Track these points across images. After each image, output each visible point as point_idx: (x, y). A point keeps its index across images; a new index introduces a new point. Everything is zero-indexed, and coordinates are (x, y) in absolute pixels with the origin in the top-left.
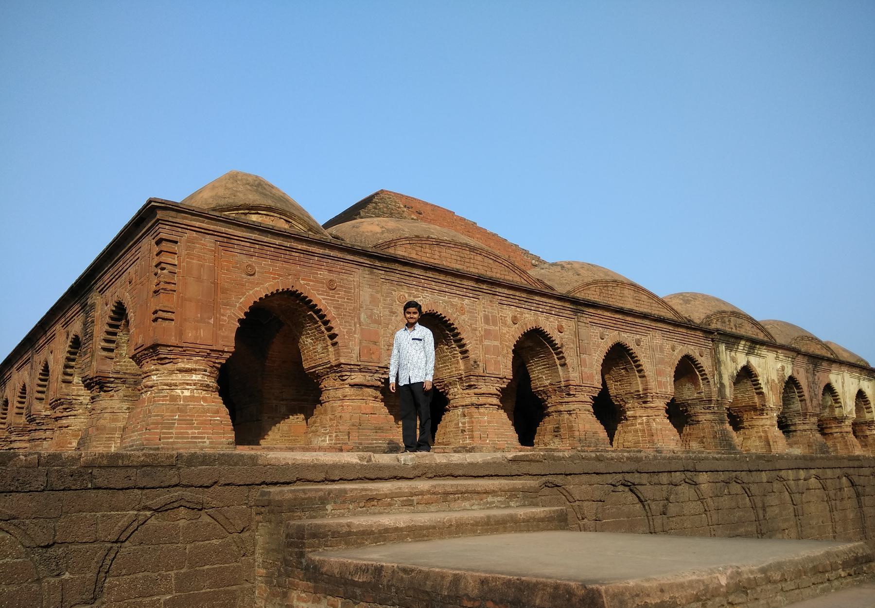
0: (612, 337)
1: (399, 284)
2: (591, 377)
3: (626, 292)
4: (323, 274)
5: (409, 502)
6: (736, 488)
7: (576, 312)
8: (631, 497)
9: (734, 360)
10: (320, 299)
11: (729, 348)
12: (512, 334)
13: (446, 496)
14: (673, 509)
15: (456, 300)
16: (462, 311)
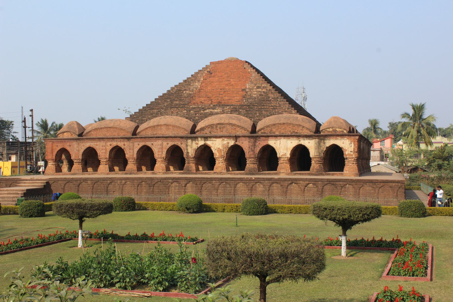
0: (142, 144)
1: (83, 143)
2: (133, 155)
3: (163, 127)
4: (68, 144)
5: (29, 183)
6: (98, 183)
7: (129, 140)
8: (71, 184)
9: (197, 144)
10: (68, 148)
11: (192, 140)
12: (109, 148)
13: (33, 183)
14: (80, 186)
15: (96, 143)
16: (97, 145)
